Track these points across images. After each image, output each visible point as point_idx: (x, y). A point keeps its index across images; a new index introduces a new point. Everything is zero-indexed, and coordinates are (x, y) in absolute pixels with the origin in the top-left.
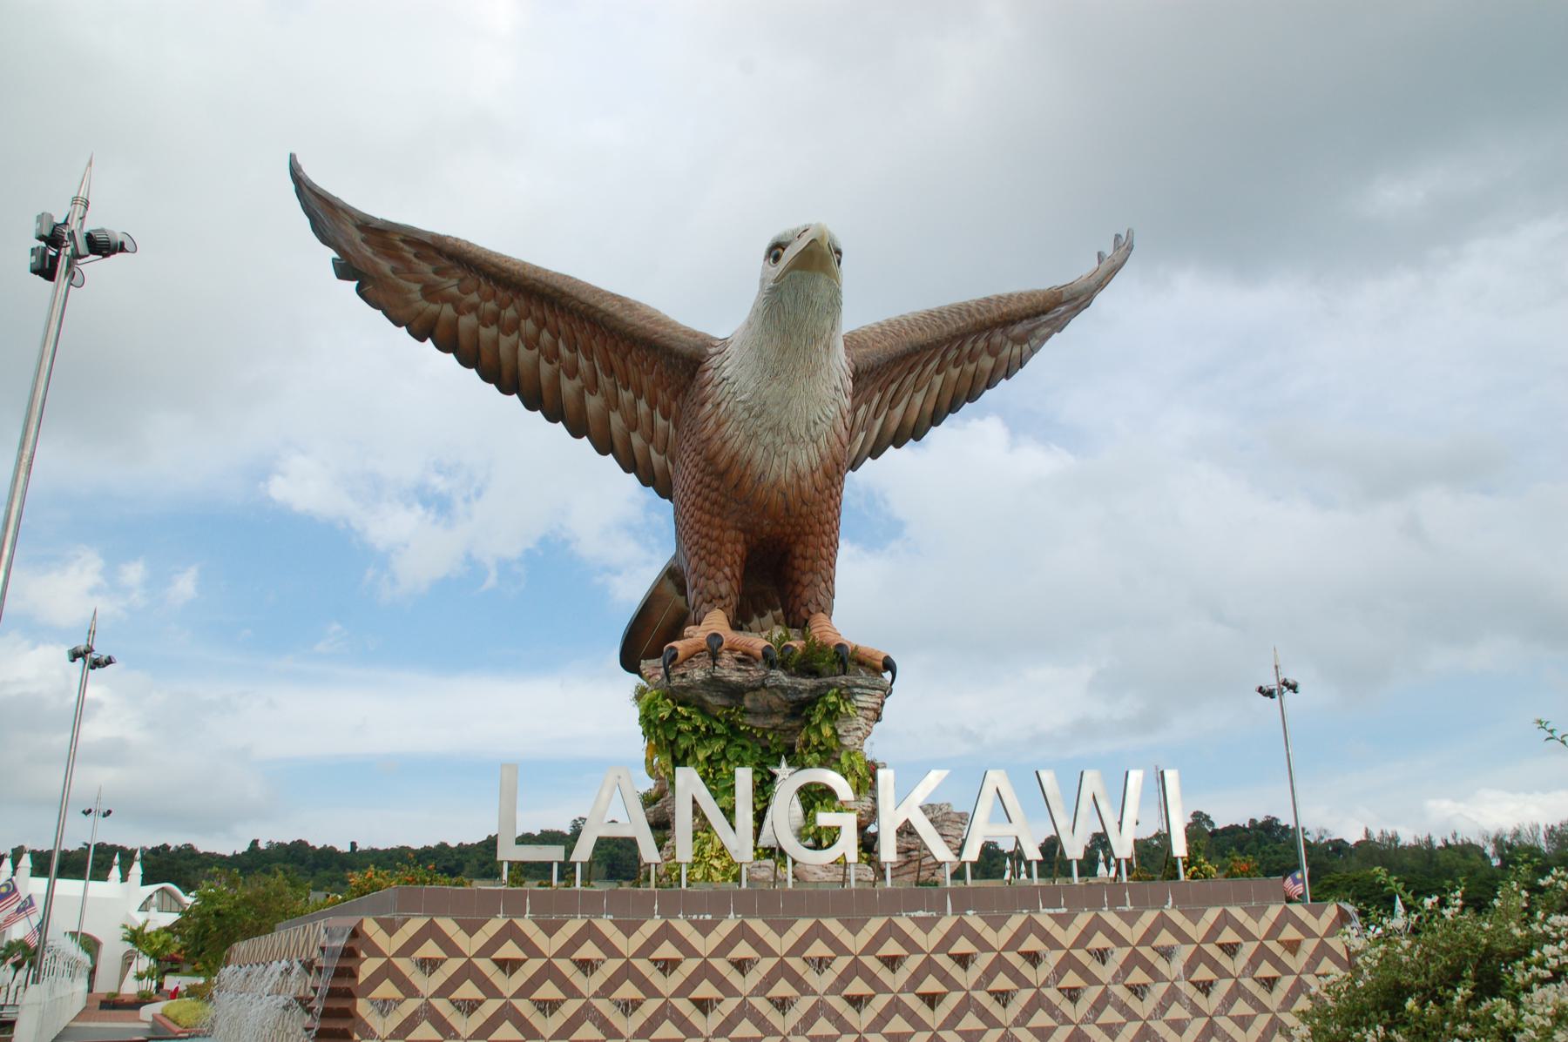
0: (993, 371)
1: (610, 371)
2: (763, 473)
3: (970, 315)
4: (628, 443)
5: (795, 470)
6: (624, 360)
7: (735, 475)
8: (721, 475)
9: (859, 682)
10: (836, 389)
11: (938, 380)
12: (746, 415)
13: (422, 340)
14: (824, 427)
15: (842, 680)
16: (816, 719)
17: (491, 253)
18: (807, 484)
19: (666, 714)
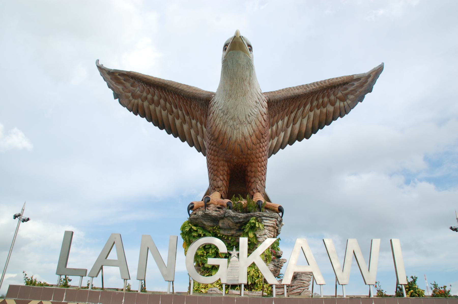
0: (334, 112)
1: (188, 114)
2: (231, 137)
3: (318, 85)
4: (197, 140)
6: (190, 108)
7: (221, 139)
8: (216, 140)
9: (265, 214)
10: (256, 102)
11: (312, 114)
12: (222, 114)
13: (136, 115)
14: (253, 118)
15: (257, 213)
16: (246, 231)
17: (143, 75)
18: (249, 141)
19: (187, 229)
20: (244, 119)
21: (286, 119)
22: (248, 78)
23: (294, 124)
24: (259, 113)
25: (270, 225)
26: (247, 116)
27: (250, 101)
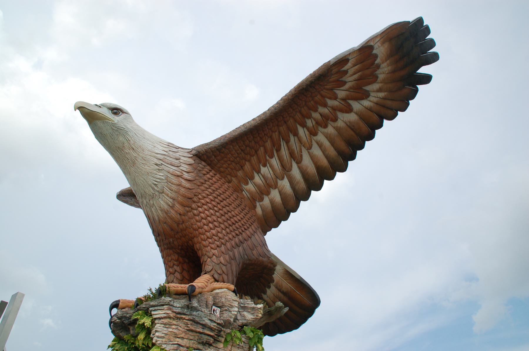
5: (161, 210)
9: (152, 303)
10: (156, 165)
11: (321, 137)
18: (173, 213)
20: (152, 191)
21: (275, 162)
22: (126, 144)
23: (299, 162)
24: (169, 175)
25: (162, 316)
26: (153, 186)
27: (146, 167)
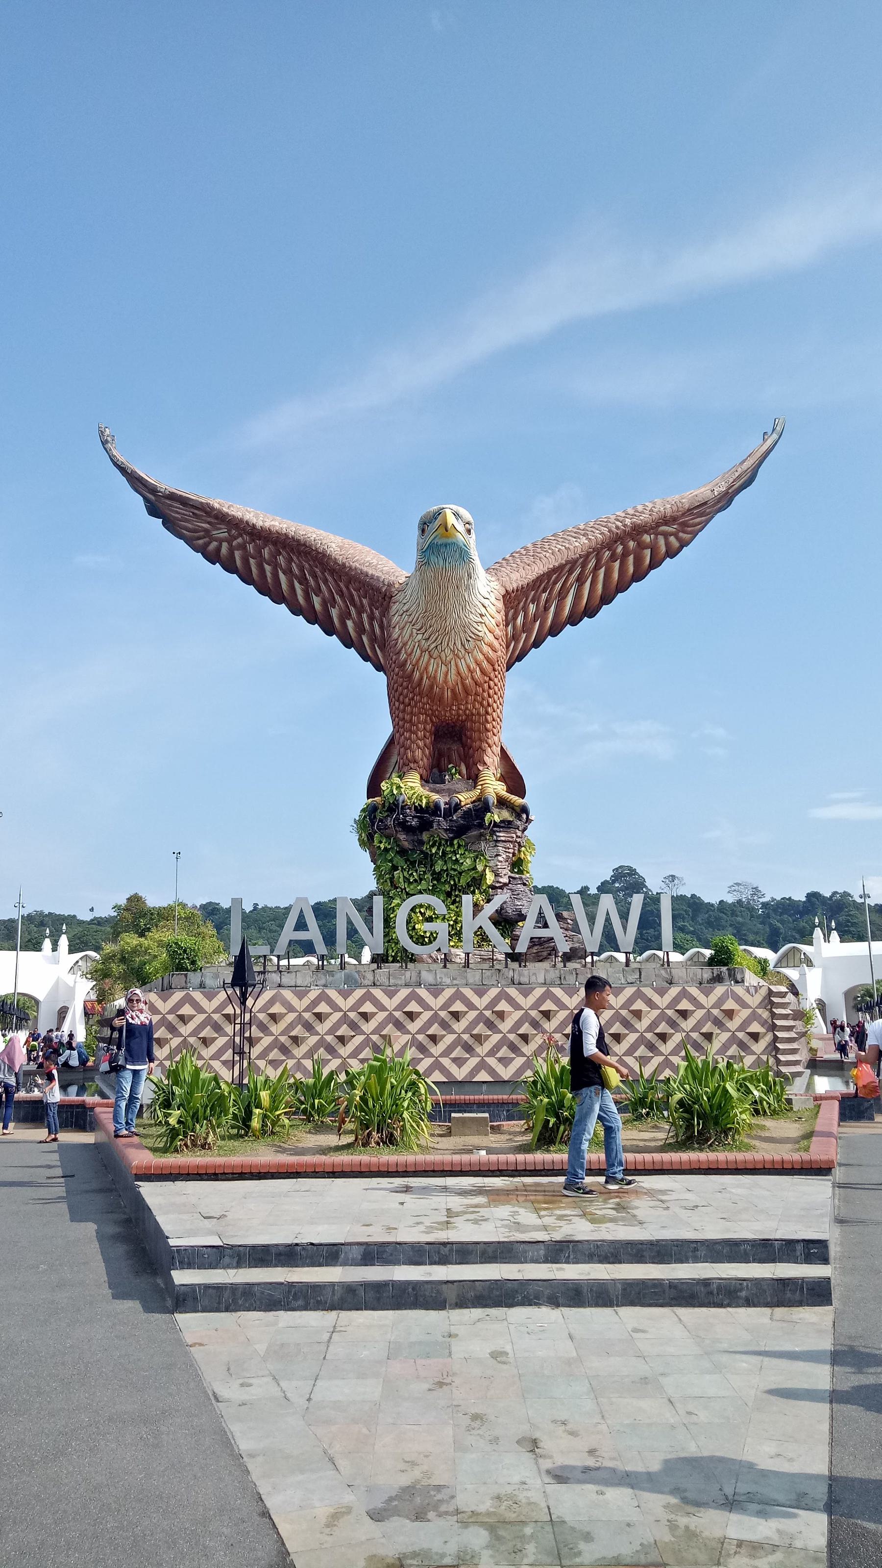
6: (348, 588)
